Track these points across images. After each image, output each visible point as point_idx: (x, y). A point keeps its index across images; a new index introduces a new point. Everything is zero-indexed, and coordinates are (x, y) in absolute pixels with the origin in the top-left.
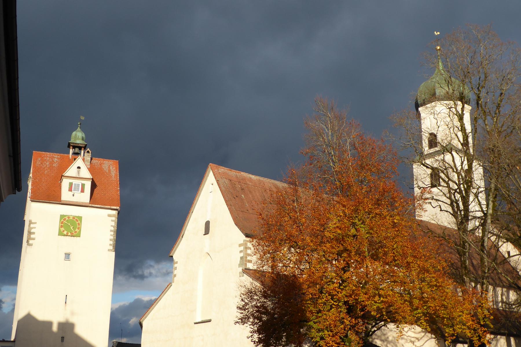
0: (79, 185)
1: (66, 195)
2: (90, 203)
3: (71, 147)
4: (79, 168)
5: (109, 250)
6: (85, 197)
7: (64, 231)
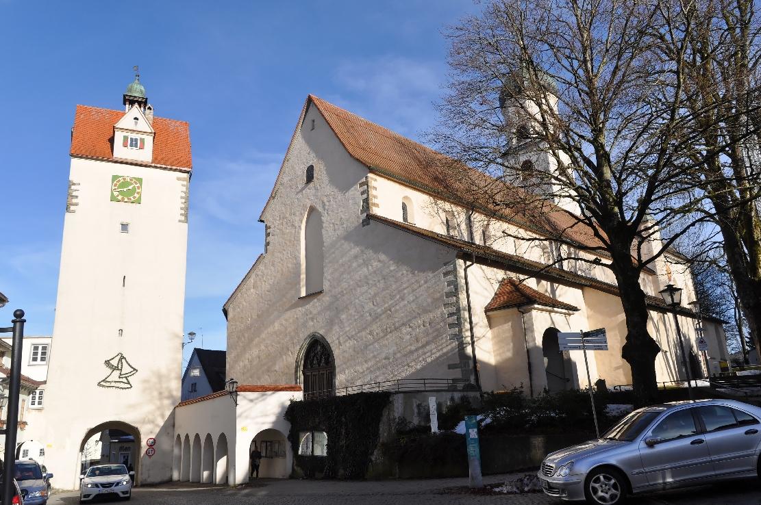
0: (136, 140)
1: (120, 151)
2: (155, 160)
3: (127, 103)
4: (136, 119)
5: (180, 221)
6: (146, 155)
7: (118, 196)
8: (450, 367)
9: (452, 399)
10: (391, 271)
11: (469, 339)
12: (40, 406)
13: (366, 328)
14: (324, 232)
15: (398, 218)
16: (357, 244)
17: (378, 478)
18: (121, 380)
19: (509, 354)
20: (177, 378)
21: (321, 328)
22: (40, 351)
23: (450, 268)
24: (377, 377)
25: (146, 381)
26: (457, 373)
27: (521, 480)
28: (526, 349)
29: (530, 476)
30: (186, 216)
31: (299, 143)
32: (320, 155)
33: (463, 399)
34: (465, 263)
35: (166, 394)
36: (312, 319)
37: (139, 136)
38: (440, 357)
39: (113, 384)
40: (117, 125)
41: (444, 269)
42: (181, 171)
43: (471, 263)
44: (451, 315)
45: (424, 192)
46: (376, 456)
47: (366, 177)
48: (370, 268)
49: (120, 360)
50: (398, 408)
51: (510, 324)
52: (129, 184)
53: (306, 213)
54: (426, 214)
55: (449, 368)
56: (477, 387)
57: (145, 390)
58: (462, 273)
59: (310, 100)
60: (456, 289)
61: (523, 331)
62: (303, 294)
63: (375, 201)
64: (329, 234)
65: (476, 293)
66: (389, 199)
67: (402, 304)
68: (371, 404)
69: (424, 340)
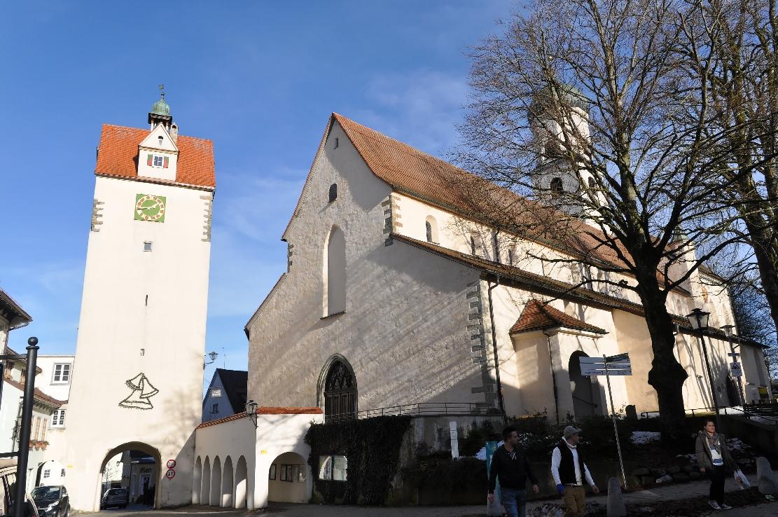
0: (161, 158)
1: (144, 170)
2: (177, 180)
3: (152, 122)
4: (160, 137)
5: (204, 240)
6: (170, 173)
7: (142, 214)
8: (474, 390)
9: (474, 424)
10: (415, 292)
11: (493, 362)
12: (62, 426)
13: (388, 349)
14: (347, 252)
15: (424, 239)
16: (380, 263)
17: (400, 504)
18: (142, 400)
19: (534, 378)
20: (198, 399)
21: (344, 348)
22: (62, 370)
23: (475, 289)
24: (399, 400)
25: (168, 401)
26: (481, 397)
27: (540, 509)
28: (551, 373)
29: (549, 504)
30: (209, 236)
31: (323, 162)
32: (343, 173)
33: (486, 424)
34: (489, 285)
35: (188, 415)
36: (334, 340)
37: (163, 155)
38: (464, 380)
39: (134, 404)
40: (143, 144)
41: (468, 290)
42: (200, 189)
43: (495, 284)
44: (474, 337)
45: (449, 212)
46: (396, 482)
47: (390, 196)
48: (392, 288)
49: (142, 380)
50: (418, 433)
51: (535, 346)
52: (152, 203)
53: (330, 232)
54: (451, 234)
55: (473, 392)
56: (501, 412)
57: (166, 410)
58: (485, 293)
59: (334, 119)
60: (480, 311)
61: (549, 354)
62: (326, 314)
63: (398, 220)
64: (353, 252)
65: (501, 314)
66: (413, 218)
67: (425, 326)
68: (392, 428)
69: (448, 363)
